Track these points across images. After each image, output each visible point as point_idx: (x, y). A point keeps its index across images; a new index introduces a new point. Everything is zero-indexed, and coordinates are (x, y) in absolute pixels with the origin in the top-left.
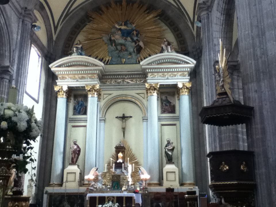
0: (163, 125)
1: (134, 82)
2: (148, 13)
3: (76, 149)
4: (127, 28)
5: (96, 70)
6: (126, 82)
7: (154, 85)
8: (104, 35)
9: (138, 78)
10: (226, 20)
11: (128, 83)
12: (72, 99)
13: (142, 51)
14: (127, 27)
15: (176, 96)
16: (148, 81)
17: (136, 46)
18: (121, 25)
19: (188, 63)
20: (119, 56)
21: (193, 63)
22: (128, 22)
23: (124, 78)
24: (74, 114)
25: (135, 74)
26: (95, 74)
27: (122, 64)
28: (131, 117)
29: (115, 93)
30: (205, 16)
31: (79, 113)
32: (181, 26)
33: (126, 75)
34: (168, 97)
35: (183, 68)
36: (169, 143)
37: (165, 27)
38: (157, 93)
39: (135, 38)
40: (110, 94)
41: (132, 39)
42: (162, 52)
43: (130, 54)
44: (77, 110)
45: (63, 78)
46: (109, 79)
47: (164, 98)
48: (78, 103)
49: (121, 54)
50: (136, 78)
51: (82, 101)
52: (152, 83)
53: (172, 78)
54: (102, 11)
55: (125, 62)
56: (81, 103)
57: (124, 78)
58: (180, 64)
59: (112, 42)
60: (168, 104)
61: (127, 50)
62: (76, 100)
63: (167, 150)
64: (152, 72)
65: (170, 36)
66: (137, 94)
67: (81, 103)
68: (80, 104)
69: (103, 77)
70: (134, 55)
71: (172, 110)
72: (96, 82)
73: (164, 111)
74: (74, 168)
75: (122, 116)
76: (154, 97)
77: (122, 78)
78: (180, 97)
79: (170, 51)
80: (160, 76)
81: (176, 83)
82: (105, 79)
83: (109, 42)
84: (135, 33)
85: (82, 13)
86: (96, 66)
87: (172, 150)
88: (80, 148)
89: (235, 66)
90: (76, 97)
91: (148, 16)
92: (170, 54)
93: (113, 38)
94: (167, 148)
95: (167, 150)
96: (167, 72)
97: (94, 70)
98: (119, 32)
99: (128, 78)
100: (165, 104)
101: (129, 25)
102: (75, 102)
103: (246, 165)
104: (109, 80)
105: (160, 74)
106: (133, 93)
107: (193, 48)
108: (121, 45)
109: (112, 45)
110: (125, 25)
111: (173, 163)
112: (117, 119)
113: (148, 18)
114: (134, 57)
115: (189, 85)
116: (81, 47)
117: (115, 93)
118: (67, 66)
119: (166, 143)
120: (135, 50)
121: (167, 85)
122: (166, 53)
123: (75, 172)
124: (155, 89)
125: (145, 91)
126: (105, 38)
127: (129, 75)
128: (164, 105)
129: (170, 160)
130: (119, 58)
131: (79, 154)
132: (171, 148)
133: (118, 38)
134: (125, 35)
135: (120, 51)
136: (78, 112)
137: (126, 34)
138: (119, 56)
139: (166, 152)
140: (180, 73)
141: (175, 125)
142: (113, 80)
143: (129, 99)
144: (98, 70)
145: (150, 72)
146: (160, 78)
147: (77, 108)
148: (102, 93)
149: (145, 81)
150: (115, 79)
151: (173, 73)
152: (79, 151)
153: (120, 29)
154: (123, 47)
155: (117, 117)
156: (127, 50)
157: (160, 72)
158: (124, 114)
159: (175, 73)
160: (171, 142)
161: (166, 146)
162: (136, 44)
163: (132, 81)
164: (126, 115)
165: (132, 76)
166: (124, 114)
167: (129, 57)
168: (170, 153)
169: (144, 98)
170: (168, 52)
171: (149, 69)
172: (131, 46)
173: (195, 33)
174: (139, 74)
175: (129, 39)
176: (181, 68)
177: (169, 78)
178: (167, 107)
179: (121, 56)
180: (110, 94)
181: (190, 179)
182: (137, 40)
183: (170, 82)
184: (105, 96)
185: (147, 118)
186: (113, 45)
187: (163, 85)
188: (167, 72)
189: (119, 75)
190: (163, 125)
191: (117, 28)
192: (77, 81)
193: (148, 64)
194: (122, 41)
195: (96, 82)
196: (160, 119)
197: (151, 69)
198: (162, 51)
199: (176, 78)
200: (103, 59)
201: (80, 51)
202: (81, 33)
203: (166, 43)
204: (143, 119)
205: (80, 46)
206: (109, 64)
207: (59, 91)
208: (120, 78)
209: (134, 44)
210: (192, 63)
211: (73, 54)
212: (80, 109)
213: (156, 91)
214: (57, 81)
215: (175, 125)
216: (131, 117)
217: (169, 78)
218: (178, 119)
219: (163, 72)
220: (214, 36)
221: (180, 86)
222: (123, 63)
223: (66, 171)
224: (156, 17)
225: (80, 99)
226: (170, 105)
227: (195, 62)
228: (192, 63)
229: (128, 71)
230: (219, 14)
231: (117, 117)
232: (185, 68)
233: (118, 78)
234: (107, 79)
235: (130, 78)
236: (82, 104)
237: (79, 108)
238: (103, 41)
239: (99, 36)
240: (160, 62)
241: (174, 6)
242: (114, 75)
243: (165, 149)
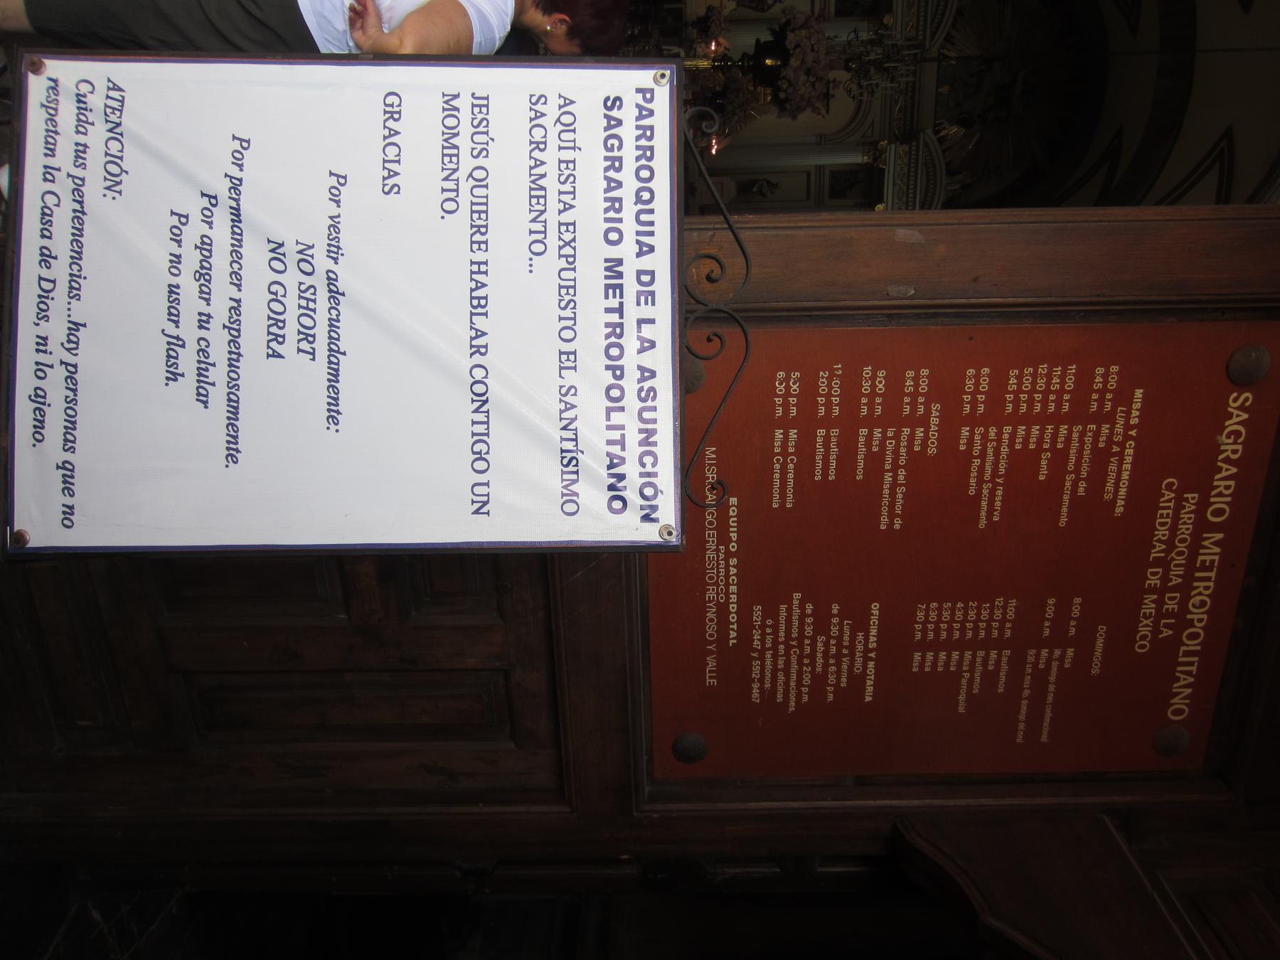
0: (809, 174)
1: (898, 115)
6: (899, 97)
7: (883, 156)
11: (897, 102)
27: (937, 88)
36: (774, 186)
38: (868, 163)
52: (888, 154)
63: (761, 183)
76: (858, 159)
79: (949, 188)
86: (933, 34)
88: (768, 10)
94: (765, 183)
95: (761, 183)
105: (906, 169)
124: (875, 160)
132: (764, 191)
141: (808, 198)
145: (910, 148)
152: (763, 10)
157: (909, 168)
159: (904, 199)
161: (768, 182)
163: (900, 110)
164: (831, 102)
168: (755, 189)
171: (918, 146)
177: (897, 187)
185: (823, 143)
190: (809, 174)
193: (926, 145)
196: (820, 168)
197: (917, 150)
198: (951, 172)
199: (896, 200)
204: (821, 136)
213: (870, 161)
215: (808, 198)
217: (897, 187)
222: (940, 90)
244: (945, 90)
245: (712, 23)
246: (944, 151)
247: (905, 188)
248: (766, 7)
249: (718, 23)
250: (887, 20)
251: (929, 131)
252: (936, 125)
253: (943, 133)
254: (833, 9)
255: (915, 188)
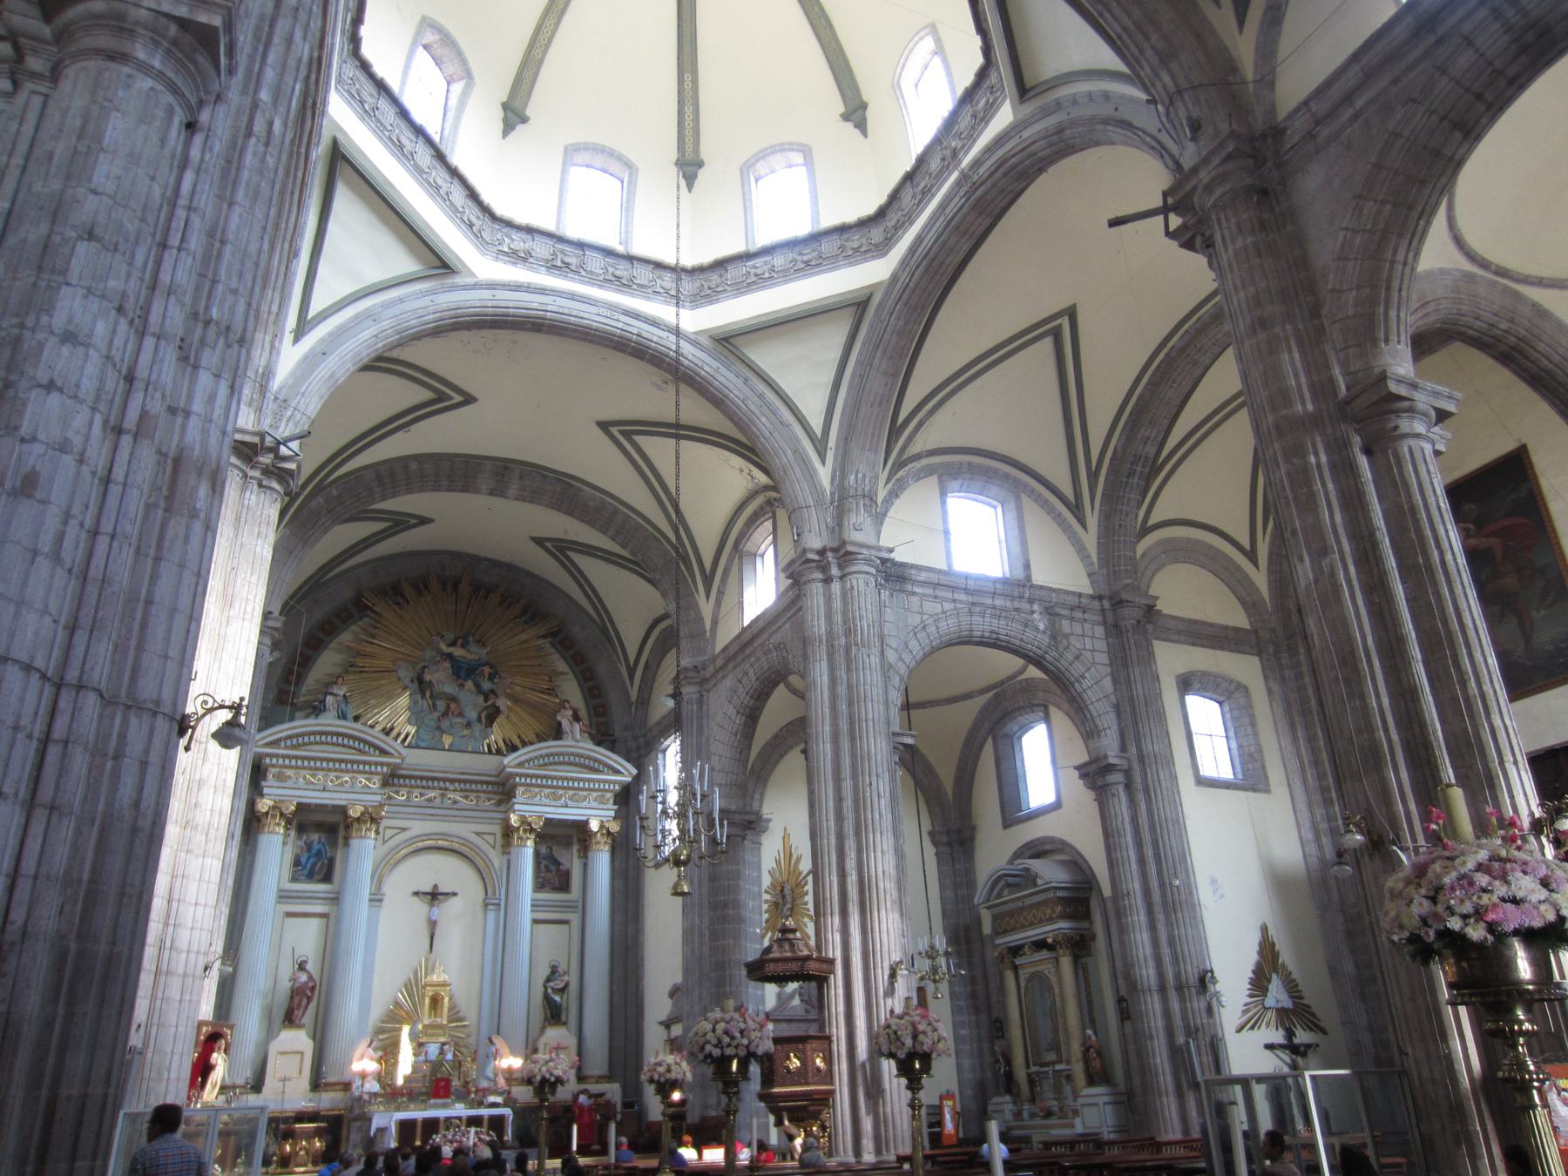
2: (526, 622)
3: (305, 984)
4: (469, 656)
5: (382, 764)
8: (404, 664)
9: (484, 792)
10: (745, 725)
11: (455, 802)
12: (293, 833)
13: (500, 719)
14: (468, 651)
15: (575, 848)
16: (517, 807)
17: (486, 708)
18: (453, 644)
19: (617, 772)
20: (439, 728)
21: (630, 774)
22: (471, 639)
23: (446, 789)
24: (294, 879)
25: (477, 782)
26: (377, 774)
27: (444, 750)
28: (455, 894)
29: (418, 827)
30: (694, 696)
31: (310, 877)
32: (601, 669)
33: (452, 781)
34: (554, 848)
35: (605, 781)
36: (554, 970)
37: (562, 666)
39: (486, 685)
40: (404, 829)
41: (477, 686)
42: (560, 739)
43: (469, 725)
44: (304, 868)
45: (280, 777)
46: (406, 786)
47: (544, 850)
48: (309, 846)
49: (446, 724)
50: (478, 791)
51: (319, 842)
52: (527, 814)
53: (576, 804)
54: (402, 596)
55: (451, 745)
56: (316, 847)
57: (446, 789)
58: (601, 772)
59: (422, 685)
60: (553, 868)
61: (461, 715)
62: (304, 838)
63: (550, 991)
64: (528, 785)
65: (571, 690)
66: (478, 834)
67: (316, 847)
68: (314, 852)
69: (392, 778)
70: (477, 728)
71: (563, 885)
72: (378, 798)
73: (541, 884)
74: (298, 1040)
75: (429, 890)
76: (527, 854)
77: (440, 789)
78: (590, 854)
80: (547, 797)
81: (584, 818)
82: (394, 785)
83: (416, 685)
84: (487, 670)
85: (347, 593)
87: (562, 990)
89: (750, 822)
90: (302, 829)
91: (523, 631)
92: (577, 741)
93: (427, 677)
94: (551, 984)
95: (550, 991)
96: (564, 788)
97: (376, 764)
98: (447, 664)
99: (455, 790)
100: (546, 867)
101: (474, 648)
102: (301, 843)
103: (824, 1059)
104: (404, 791)
106: (464, 830)
107: (626, 729)
108: (453, 699)
109: (423, 696)
110: (463, 646)
111: (565, 1024)
112: (416, 899)
113: (524, 636)
114: (477, 734)
115: (615, 827)
116: (344, 696)
117: (418, 827)
118: (294, 747)
119: (547, 971)
120: (484, 714)
121: (560, 820)
122: (569, 742)
123: (301, 1049)
124: (532, 830)
125: (497, 829)
126: (405, 674)
127: (460, 781)
128: (542, 866)
129: (554, 1014)
130: (437, 733)
131: (309, 999)
133: (440, 677)
134: (463, 673)
135: (445, 714)
136: (306, 872)
137: (463, 671)
138: (439, 728)
139: (546, 996)
140: (595, 794)
142: (416, 792)
143: (456, 846)
144: (388, 764)
145: (522, 785)
146: (547, 801)
147: (303, 860)
148: (384, 823)
149: (511, 809)
150: (423, 787)
151: (577, 792)
152: (313, 989)
153: (450, 657)
154: (453, 706)
155: (416, 894)
156: (461, 715)
157: (549, 787)
158: (436, 886)
159: (585, 793)
160: (560, 970)
161: (548, 980)
162: (486, 701)
163: (466, 798)
164: (442, 890)
165: (466, 783)
166: (436, 886)
167: (466, 732)
168: (557, 998)
169: (494, 848)
170: (573, 738)
171: (521, 775)
172: (472, 705)
173: (634, 694)
174: (487, 783)
175: (469, 684)
176: (599, 781)
177: (570, 803)
178: (549, 875)
179: (444, 727)
180: (404, 829)
181: (598, 1062)
182: (492, 691)
183: (571, 813)
184: (389, 833)
186: (428, 694)
187: (551, 820)
188: (564, 788)
189: (433, 779)
190: (536, 921)
191: (443, 654)
192: (324, 790)
193: (520, 765)
194: (449, 688)
195: (378, 798)
196: (535, 906)
197: (527, 776)
198: (558, 733)
199: (585, 804)
200: (392, 729)
201: (343, 706)
202: (333, 645)
203: (570, 713)
204: (486, 905)
205: (341, 693)
206: (409, 746)
207: (267, 813)
208: (434, 788)
209: (481, 698)
210: (627, 772)
211: (326, 714)
212: (314, 865)
213: (533, 836)
214: (263, 783)
216: (455, 894)
217: (570, 803)
218: (583, 908)
219: (553, 787)
220: (713, 748)
221: (594, 825)
223: (274, 1047)
224: (545, 637)
225: (315, 837)
226: (558, 870)
227: (634, 771)
228: (627, 772)
229: (463, 773)
230: (732, 711)
231: (416, 894)
232: (609, 782)
233: (428, 788)
234: (400, 786)
235: (461, 790)
236: (319, 853)
237: (311, 861)
238: (399, 679)
239: (388, 664)
240: (548, 761)
241: (587, 614)
242: (422, 778)
243: (546, 988)
244: (447, 740)
245: (551, 1074)
246: (524, 744)
247: (571, 792)
248: (311, 984)
249: (551, 1064)
250: (355, 812)
251: (506, 761)
252: (490, 752)
253: (502, 744)
254: (322, 887)
255: (574, 780)
